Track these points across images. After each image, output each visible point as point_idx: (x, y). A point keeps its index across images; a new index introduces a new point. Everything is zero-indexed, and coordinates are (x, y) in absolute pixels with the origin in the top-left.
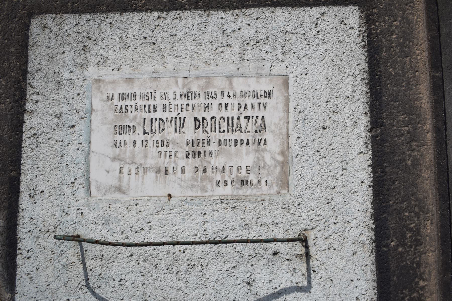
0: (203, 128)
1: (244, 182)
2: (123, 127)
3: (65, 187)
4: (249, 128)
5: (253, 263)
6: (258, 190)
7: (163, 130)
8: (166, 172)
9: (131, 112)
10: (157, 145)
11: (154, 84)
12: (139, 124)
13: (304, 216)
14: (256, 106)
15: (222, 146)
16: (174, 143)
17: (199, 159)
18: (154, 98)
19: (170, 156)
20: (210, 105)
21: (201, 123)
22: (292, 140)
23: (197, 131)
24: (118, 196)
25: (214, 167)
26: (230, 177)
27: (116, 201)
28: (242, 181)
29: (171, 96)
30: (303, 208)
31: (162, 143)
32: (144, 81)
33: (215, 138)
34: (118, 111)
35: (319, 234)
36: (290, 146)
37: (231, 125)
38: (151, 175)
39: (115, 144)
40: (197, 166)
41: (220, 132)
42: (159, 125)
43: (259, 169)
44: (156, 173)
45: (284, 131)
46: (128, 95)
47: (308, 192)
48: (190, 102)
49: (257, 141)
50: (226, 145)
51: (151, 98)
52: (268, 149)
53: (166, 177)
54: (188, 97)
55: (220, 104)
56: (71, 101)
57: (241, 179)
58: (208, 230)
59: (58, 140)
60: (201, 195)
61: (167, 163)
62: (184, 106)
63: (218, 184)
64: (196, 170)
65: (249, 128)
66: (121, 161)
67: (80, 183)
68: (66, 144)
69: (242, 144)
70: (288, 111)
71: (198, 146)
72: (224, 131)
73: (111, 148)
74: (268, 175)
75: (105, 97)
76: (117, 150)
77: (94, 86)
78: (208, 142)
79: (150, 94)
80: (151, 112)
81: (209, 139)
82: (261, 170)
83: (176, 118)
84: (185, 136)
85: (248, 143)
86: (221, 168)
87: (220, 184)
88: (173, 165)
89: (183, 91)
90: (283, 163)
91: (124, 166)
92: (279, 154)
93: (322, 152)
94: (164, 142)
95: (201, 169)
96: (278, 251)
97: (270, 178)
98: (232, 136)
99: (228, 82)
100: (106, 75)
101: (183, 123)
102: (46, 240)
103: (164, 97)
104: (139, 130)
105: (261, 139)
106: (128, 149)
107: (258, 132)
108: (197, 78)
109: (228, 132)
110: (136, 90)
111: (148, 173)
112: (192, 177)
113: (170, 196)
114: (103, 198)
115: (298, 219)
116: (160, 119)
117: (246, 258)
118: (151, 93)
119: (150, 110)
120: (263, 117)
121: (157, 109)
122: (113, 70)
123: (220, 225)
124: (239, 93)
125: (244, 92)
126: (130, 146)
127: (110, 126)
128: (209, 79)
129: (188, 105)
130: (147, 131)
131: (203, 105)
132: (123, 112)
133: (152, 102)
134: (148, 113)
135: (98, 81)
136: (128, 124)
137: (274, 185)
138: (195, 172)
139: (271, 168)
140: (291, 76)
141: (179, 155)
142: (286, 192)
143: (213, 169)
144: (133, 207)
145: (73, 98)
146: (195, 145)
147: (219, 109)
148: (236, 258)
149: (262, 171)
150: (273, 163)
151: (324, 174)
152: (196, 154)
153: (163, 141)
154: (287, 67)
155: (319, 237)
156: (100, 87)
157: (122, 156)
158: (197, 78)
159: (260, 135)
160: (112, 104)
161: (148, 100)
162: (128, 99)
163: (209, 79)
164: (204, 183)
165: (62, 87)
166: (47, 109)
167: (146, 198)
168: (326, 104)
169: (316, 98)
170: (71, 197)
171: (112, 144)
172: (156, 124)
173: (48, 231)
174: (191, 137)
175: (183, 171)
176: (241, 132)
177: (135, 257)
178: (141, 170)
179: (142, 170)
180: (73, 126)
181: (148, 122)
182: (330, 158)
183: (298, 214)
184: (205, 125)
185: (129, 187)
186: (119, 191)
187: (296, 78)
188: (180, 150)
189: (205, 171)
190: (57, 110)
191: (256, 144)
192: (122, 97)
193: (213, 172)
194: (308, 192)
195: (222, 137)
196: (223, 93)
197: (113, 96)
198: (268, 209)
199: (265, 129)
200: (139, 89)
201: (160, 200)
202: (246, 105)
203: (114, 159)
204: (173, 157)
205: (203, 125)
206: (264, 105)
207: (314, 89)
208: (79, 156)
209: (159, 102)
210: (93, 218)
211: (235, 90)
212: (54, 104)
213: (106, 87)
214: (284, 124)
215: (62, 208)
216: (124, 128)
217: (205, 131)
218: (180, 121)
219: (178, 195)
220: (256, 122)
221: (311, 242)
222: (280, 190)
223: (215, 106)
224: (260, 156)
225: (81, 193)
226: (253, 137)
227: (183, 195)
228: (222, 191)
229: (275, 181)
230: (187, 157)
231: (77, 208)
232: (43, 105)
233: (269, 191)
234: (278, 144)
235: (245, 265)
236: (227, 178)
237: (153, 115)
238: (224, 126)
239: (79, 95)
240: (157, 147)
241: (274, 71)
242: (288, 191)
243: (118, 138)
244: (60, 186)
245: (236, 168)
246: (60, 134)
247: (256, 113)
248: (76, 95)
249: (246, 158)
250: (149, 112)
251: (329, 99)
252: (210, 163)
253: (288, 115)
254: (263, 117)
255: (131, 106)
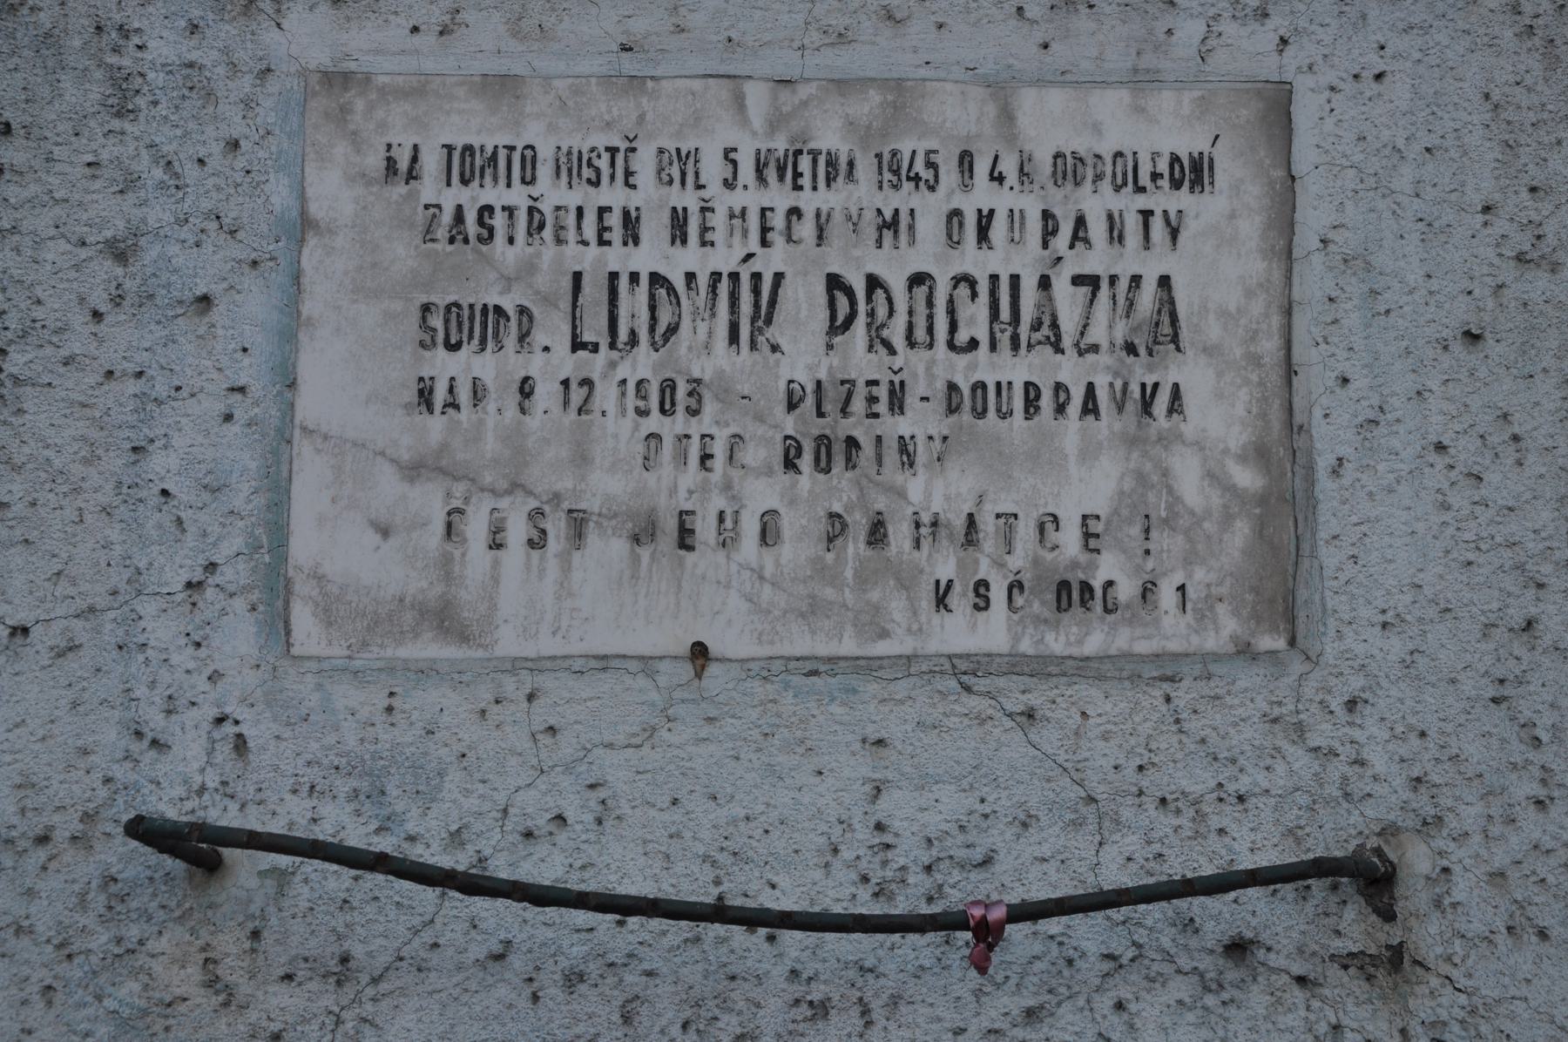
0: (869, 325)
1: (1072, 594)
2: (466, 313)
3: (148, 608)
4: (1097, 334)
5: (1125, 993)
6: (1139, 632)
7: (673, 329)
8: (685, 538)
9: (511, 241)
10: (641, 404)
11: (625, 110)
12: (548, 301)
13: (1379, 761)
14: (1132, 224)
15: (966, 416)
16: (725, 394)
17: (849, 474)
18: (628, 174)
19: (706, 457)
20: (904, 220)
21: (862, 307)
22: (1314, 381)
23: (838, 340)
24: (429, 649)
25: (926, 518)
26: (1000, 565)
27: (425, 672)
28: (1064, 586)
29: (712, 169)
30: (1371, 728)
31: (662, 392)
32: (577, 91)
33: (931, 376)
34: (442, 233)
35: (1459, 855)
36: (1299, 418)
37: (1005, 314)
38: (607, 549)
39: (425, 396)
40: (837, 508)
41: (951, 345)
42: (653, 308)
43: (1147, 531)
44: (636, 539)
45: (1270, 346)
46: (494, 158)
47: (1396, 646)
48: (809, 201)
49: (1137, 394)
50: (985, 410)
51: (612, 177)
52: (1188, 429)
53: (681, 564)
54: (797, 175)
55: (956, 213)
56: (191, 172)
57: (1058, 578)
58: (896, 824)
59: (118, 369)
60: (859, 653)
61: (691, 492)
62: (778, 221)
63: (941, 599)
64: (836, 527)
65: (1097, 334)
66: (456, 479)
67: (232, 588)
68: (161, 389)
69: (1060, 409)
70: (1290, 252)
71: (844, 412)
72: (973, 344)
73: (400, 412)
74: (1189, 560)
75: (374, 161)
76: (436, 425)
77: (313, 104)
78: (892, 392)
79: (606, 156)
80: (609, 243)
81: (897, 379)
82: (1154, 534)
83: (734, 277)
84: (777, 363)
85: (1090, 407)
86: (960, 523)
87: (953, 600)
88: (718, 502)
89: (772, 145)
90: (1263, 500)
91: (467, 500)
92: (1242, 459)
93: (1465, 451)
94: (673, 388)
95: (859, 523)
96: (1249, 935)
97: (1200, 574)
98: (1016, 370)
99: (991, 110)
100: (377, 52)
101: (773, 302)
102: (28, 883)
103: (675, 172)
104: (553, 330)
105: (1156, 385)
106: (491, 422)
107: (1142, 351)
108: (842, 85)
109: (993, 346)
110: (533, 133)
111: (592, 538)
112: (816, 562)
113: (700, 652)
114: (358, 663)
115: (1345, 778)
116: (656, 279)
117: (1091, 968)
118: (613, 151)
119: (606, 236)
120: (1164, 281)
121: (645, 233)
122: (415, 29)
123: (951, 803)
124: (1050, 160)
125: (1070, 160)
126: (501, 409)
127: (397, 306)
128: (900, 93)
129: (795, 212)
130: (588, 337)
131: (869, 215)
132: (466, 241)
133: (613, 196)
134: (594, 250)
135: (337, 80)
136: (493, 299)
137: (1222, 609)
138: (830, 540)
139: (1206, 525)
140: (1302, 84)
141: (752, 455)
142: (1280, 643)
143: (918, 525)
144: (513, 707)
145: (201, 161)
146: (827, 407)
147: (950, 236)
148: (1039, 966)
149: (1160, 540)
150: (1216, 500)
151: (1471, 556)
152: (833, 452)
153: (668, 386)
154: (1284, 41)
155: (1457, 869)
156: (345, 110)
157: (460, 456)
158: (842, 85)
159: (1150, 368)
160: (412, 196)
161: (595, 183)
162: (495, 179)
163: (900, 93)
164: (875, 595)
165: (141, 102)
166: (57, 210)
167: (578, 664)
168: (1480, 218)
169: (1429, 193)
170: (183, 658)
171: (411, 395)
172: (633, 305)
173: (43, 840)
174: (810, 368)
175: (768, 534)
176: (1059, 350)
177: (517, 961)
178: (557, 527)
179: (563, 524)
180: (205, 300)
181: (594, 292)
182: (1502, 483)
183: (1347, 752)
184: (882, 312)
185: (493, 607)
186: (440, 626)
187: (1327, 93)
188: (751, 429)
189: (877, 533)
190: (109, 213)
191: (1132, 407)
192: (467, 164)
193: (917, 544)
194: (1396, 646)
195: (964, 371)
196: (966, 161)
197: (415, 159)
198: (1193, 725)
199: (1175, 339)
200: (552, 128)
201: (651, 674)
202: (1080, 222)
203: (413, 471)
204: (719, 463)
205: (871, 314)
206: (1168, 222)
207: (1418, 147)
208: (240, 455)
209: (650, 197)
210: (300, 762)
211: (1027, 148)
212: (98, 184)
213: (380, 114)
214: (1267, 315)
215: (132, 714)
216: (472, 318)
217: (879, 341)
218: (756, 291)
219: (743, 654)
220: (1131, 304)
221: (1412, 895)
222: (1253, 634)
223: (930, 226)
224: (1148, 466)
225: (238, 637)
226: (1116, 374)
227: (766, 651)
228: (959, 632)
229: (1223, 590)
230: (790, 464)
231: (214, 712)
232: (34, 189)
233: (1195, 640)
234: (1240, 410)
235: (1081, 1002)
236: (984, 570)
237: (618, 258)
238: (972, 321)
239: (234, 145)
240: (643, 413)
241: (1220, 60)
242: (1292, 642)
243: (443, 366)
244: (121, 598)
245: (1032, 524)
246: (125, 338)
247: (1130, 260)
248: (216, 148)
249: (1084, 476)
250: (602, 242)
251: (1497, 196)
252: (902, 494)
253: (1290, 270)
254: (1164, 281)
255: (510, 211)
